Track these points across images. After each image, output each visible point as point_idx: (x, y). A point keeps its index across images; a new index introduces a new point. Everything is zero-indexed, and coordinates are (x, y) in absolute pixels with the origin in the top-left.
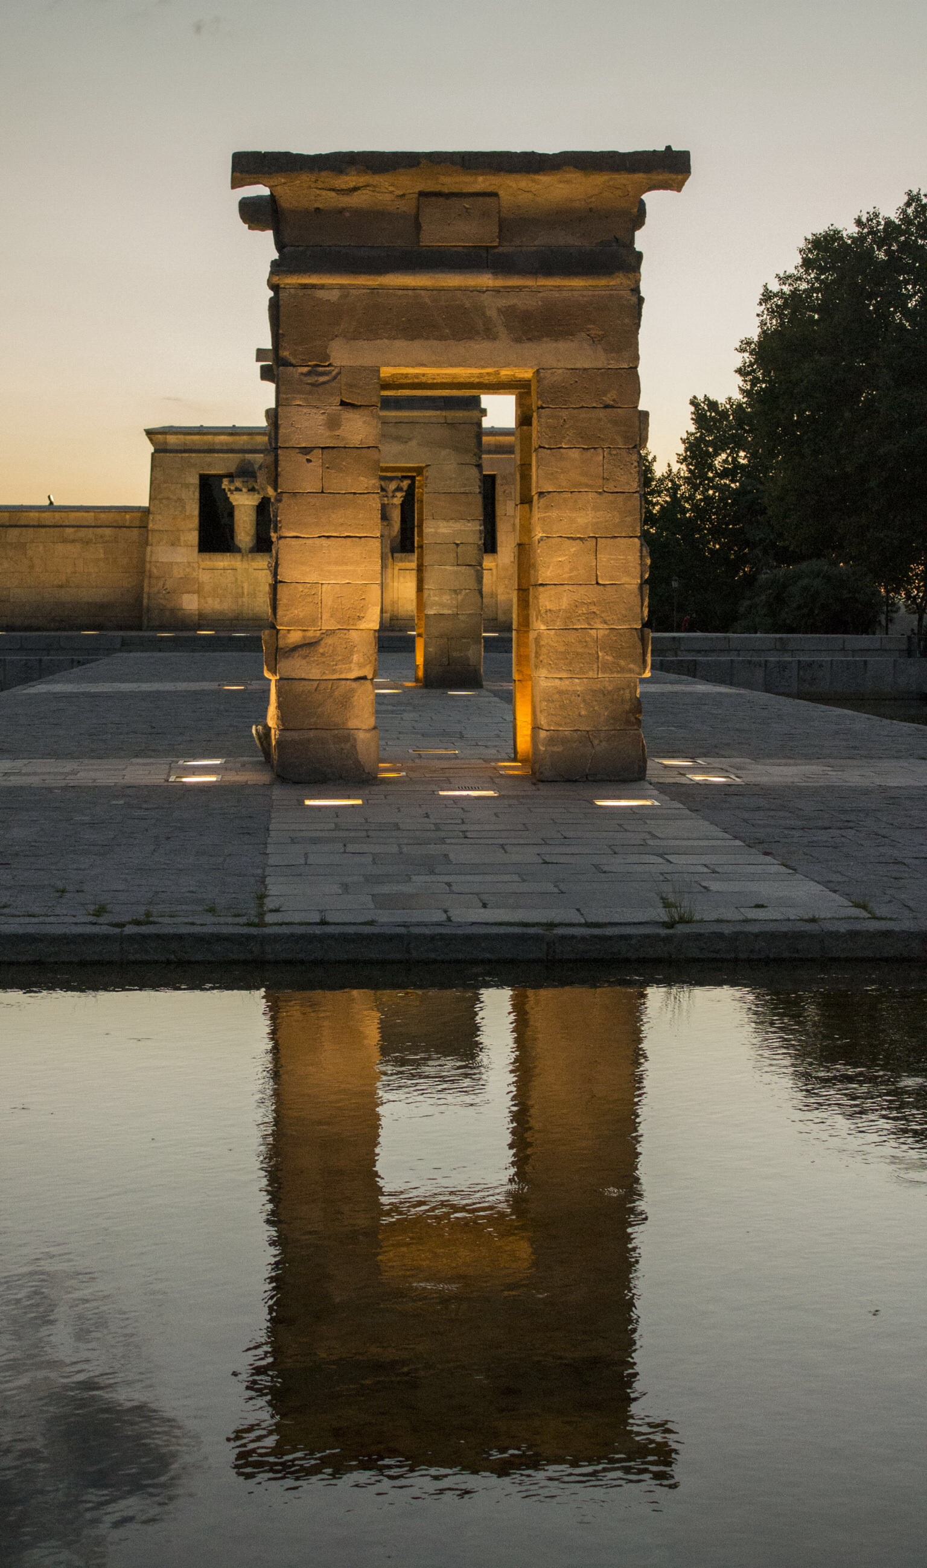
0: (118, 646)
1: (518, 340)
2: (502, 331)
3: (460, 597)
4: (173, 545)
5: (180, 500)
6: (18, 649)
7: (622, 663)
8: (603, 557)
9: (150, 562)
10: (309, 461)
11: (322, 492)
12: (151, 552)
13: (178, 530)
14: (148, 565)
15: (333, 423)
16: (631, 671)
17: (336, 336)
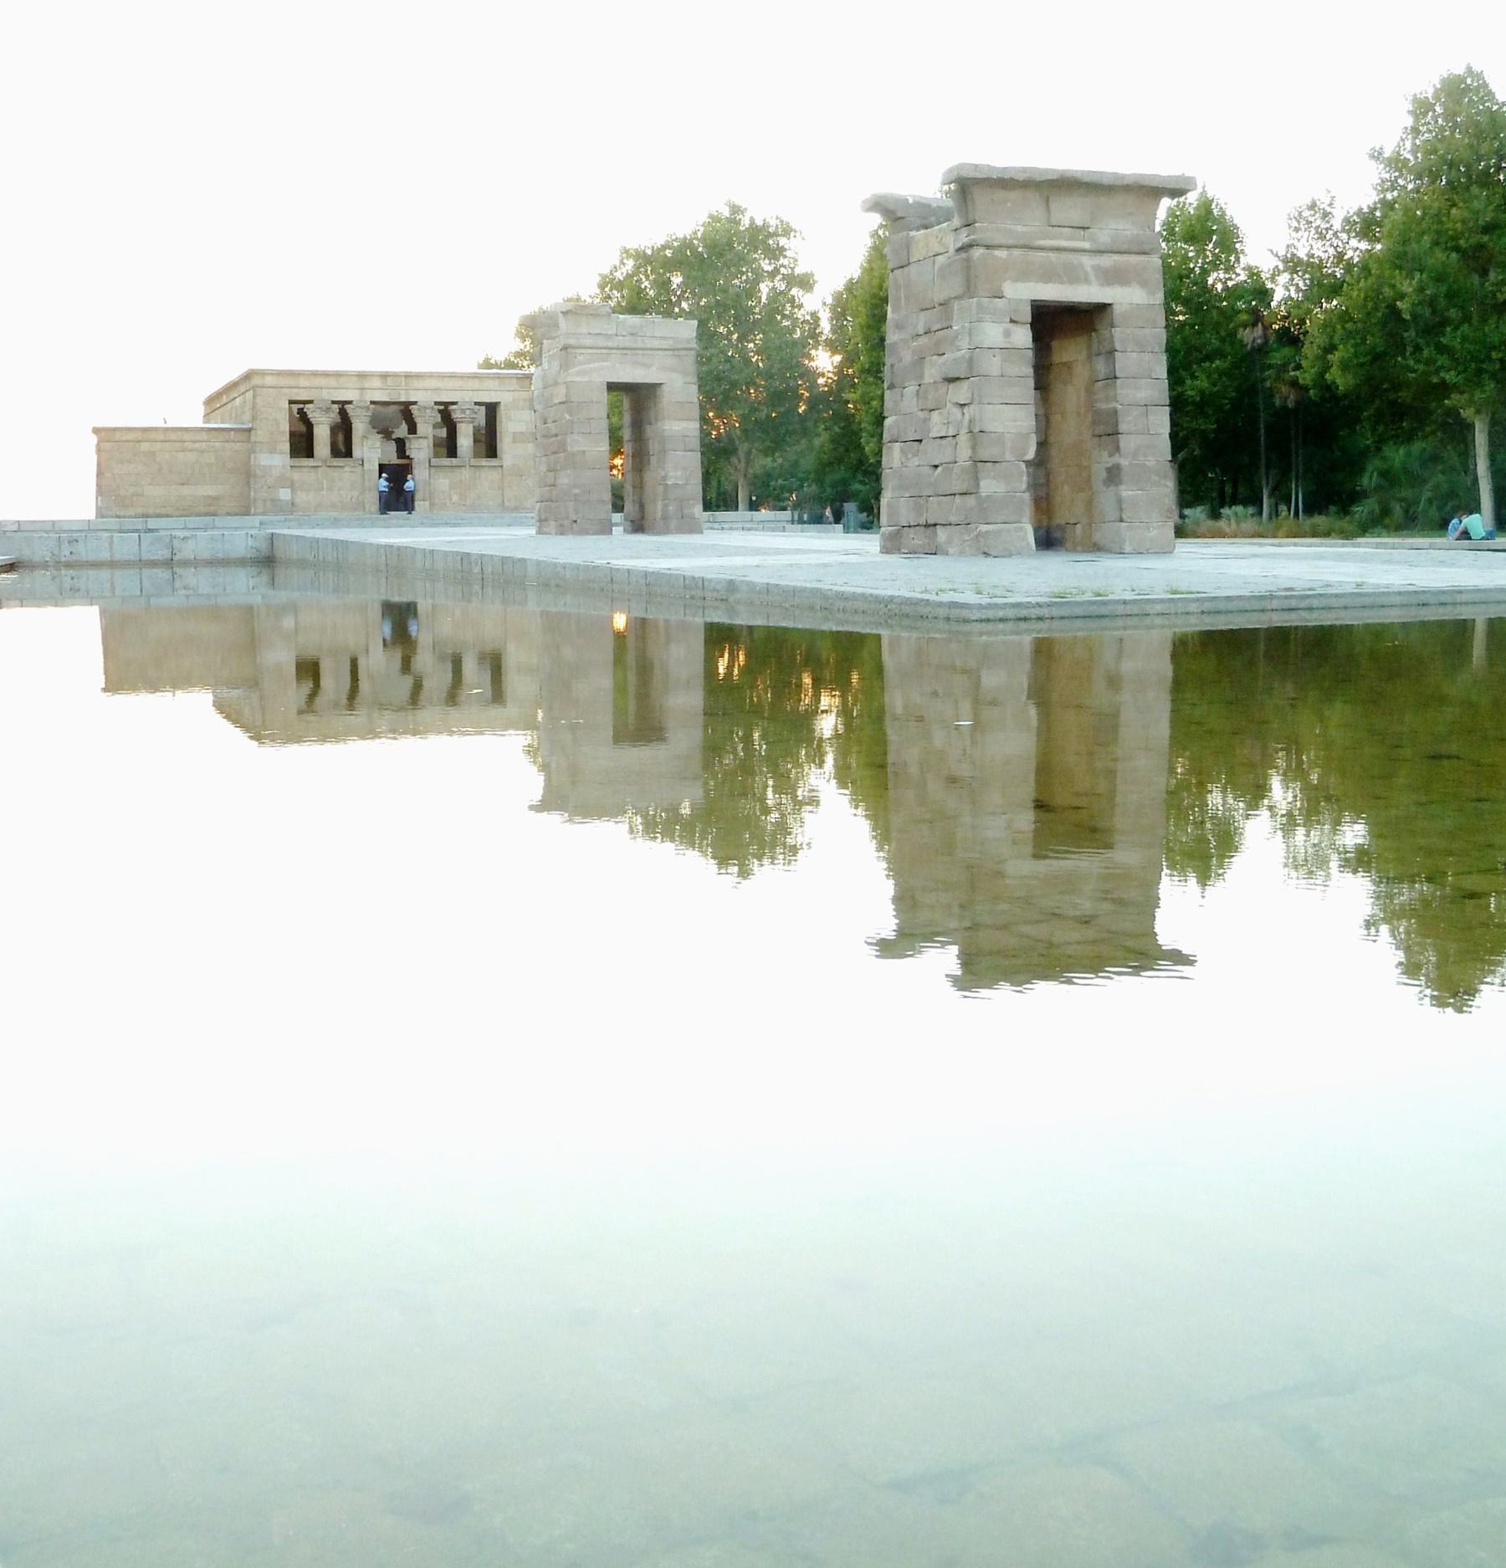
0: (258, 525)
1: (1103, 285)
2: (1092, 278)
3: (688, 473)
4: (271, 453)
5: (275, 420)
6: (183, 529)
7: (1163, 482)
8: (1151, 418)
9: (255, 465)
10: (994, 356)
11: (1002, 376)
12: (255, 458)
13: (275, 442)
14: (252, 468)
15: (1007, 334)
16: (1167, 486)
17: (1006, 280)
